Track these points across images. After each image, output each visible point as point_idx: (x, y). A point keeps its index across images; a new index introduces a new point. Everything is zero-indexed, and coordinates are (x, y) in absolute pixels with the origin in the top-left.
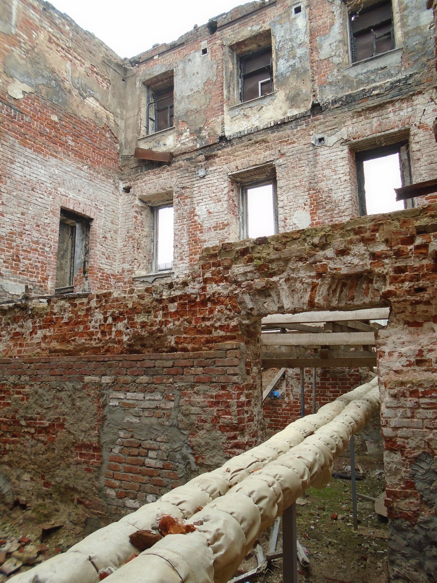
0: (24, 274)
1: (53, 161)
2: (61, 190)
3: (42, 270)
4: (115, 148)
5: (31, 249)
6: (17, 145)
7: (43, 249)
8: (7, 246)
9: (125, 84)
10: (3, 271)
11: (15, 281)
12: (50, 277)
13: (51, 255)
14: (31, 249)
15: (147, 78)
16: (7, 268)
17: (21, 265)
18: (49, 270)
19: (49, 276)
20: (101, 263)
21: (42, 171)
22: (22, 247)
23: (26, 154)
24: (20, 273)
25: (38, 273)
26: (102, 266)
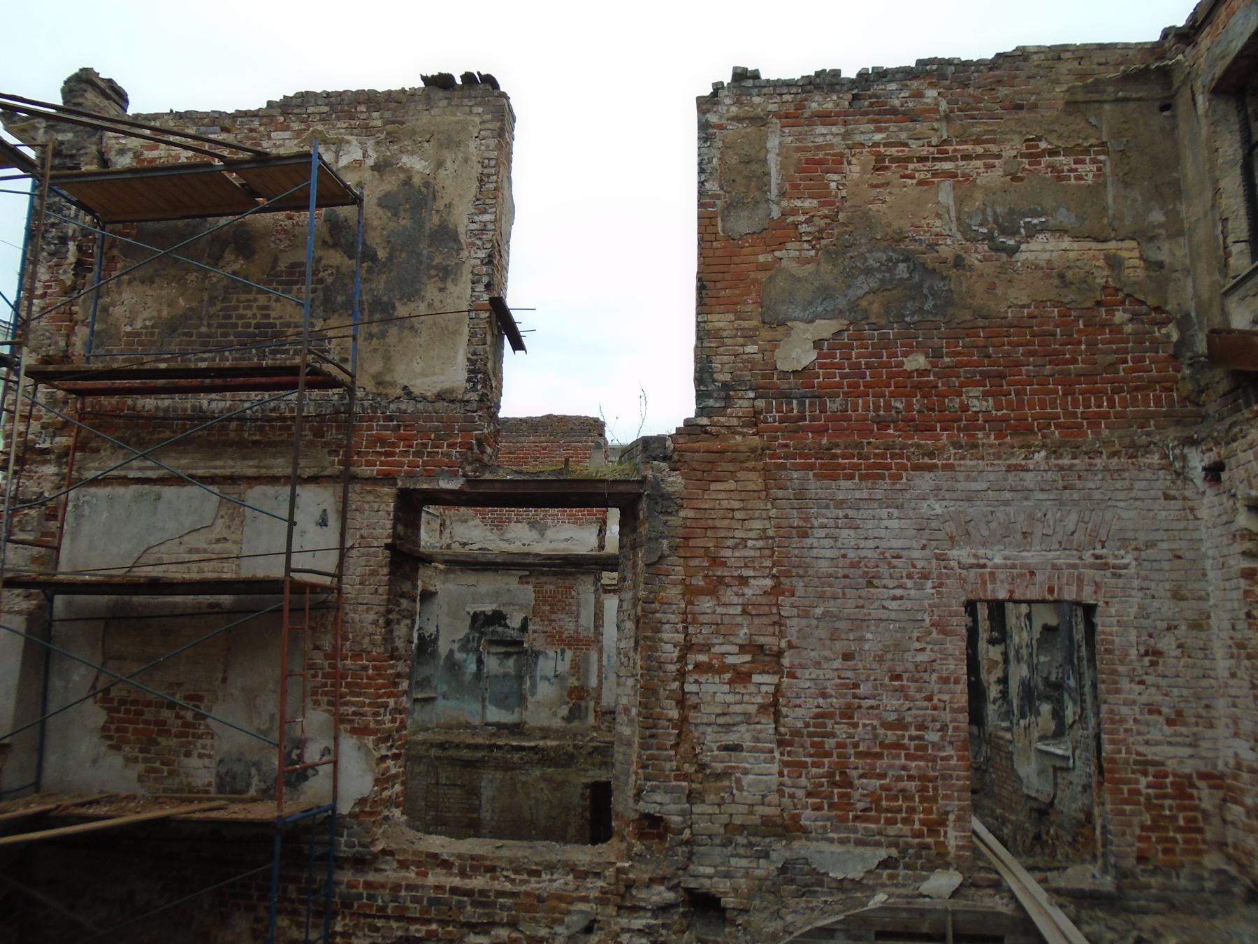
0: (868, 820)
1: (925, 481)
2: (961, 554)
3: (923, 800)
5: (882, 745)
6: (813, 484)
7: (921, 738)
8: (812, 751)
9: (1174, 117)
10: (808, 819)
11: (842, 842)
12: (952, 817)
13: (949, 751)
14: (882, 745)
15: (1219, 70)
16: (818, 808)
17: (856, 795)
18: (946, 797)
19: (947, 813)
20: (1147, 743)
21: (894, 524)
22: (856, 745)
23: (840, 496)
24: (856, 818)
25: (912, 810)
26: (1151, 753)
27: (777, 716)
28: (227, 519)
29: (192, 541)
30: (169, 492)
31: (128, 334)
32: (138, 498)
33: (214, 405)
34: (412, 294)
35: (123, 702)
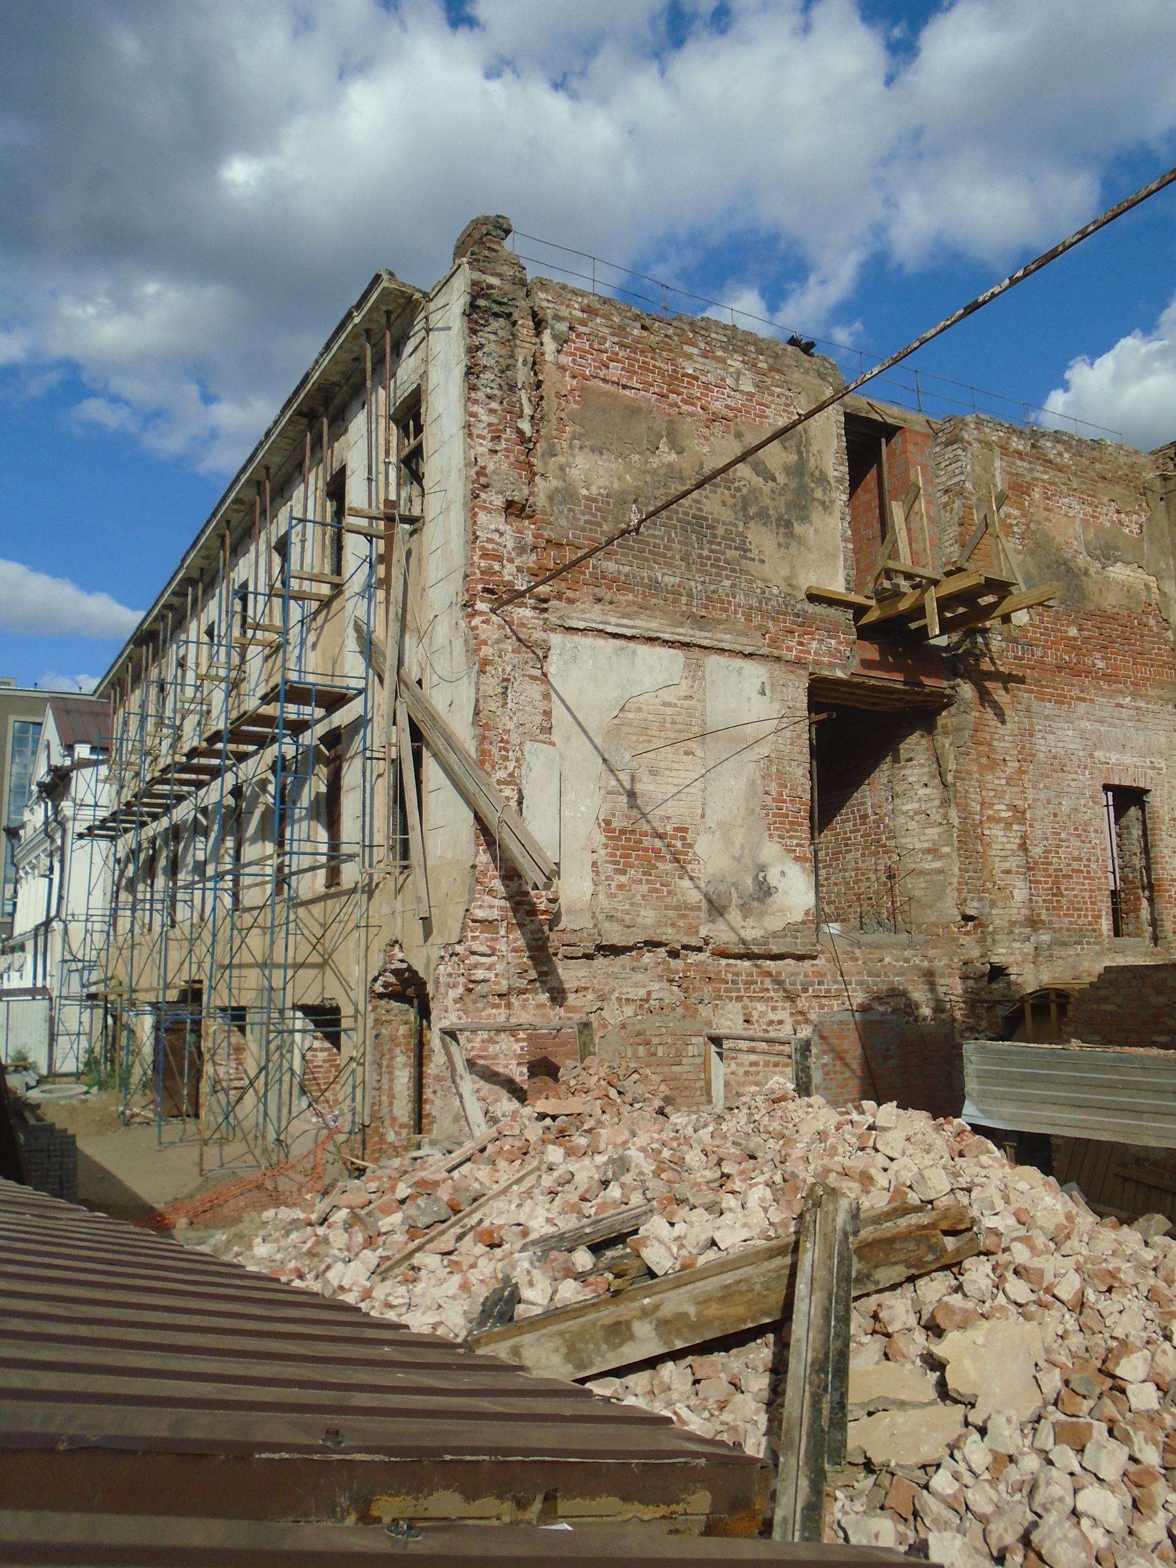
1: (1082, 707)
2: (1099, 754)
4: (1166, 642)
6: (1035, 703)
17: (1064, 901)
21: (1070, 733)
23: (1047, 712)
27: (1026, 850)
28: (689, 681)
29: (666, 695)
30: (643, 650)
31: (587, 498)
32: (616, 651)
33: (666, 578)
34: (805, 519)
35: (623, 832)
